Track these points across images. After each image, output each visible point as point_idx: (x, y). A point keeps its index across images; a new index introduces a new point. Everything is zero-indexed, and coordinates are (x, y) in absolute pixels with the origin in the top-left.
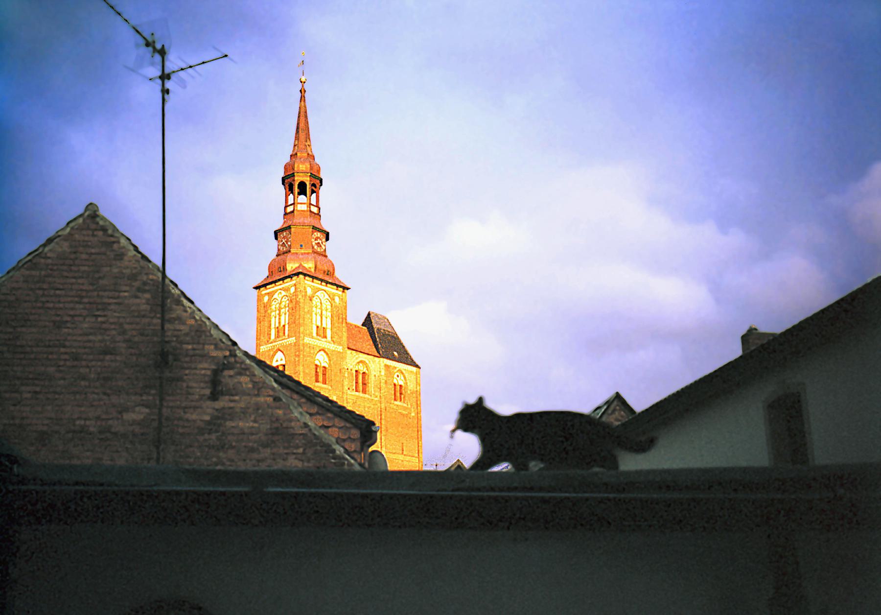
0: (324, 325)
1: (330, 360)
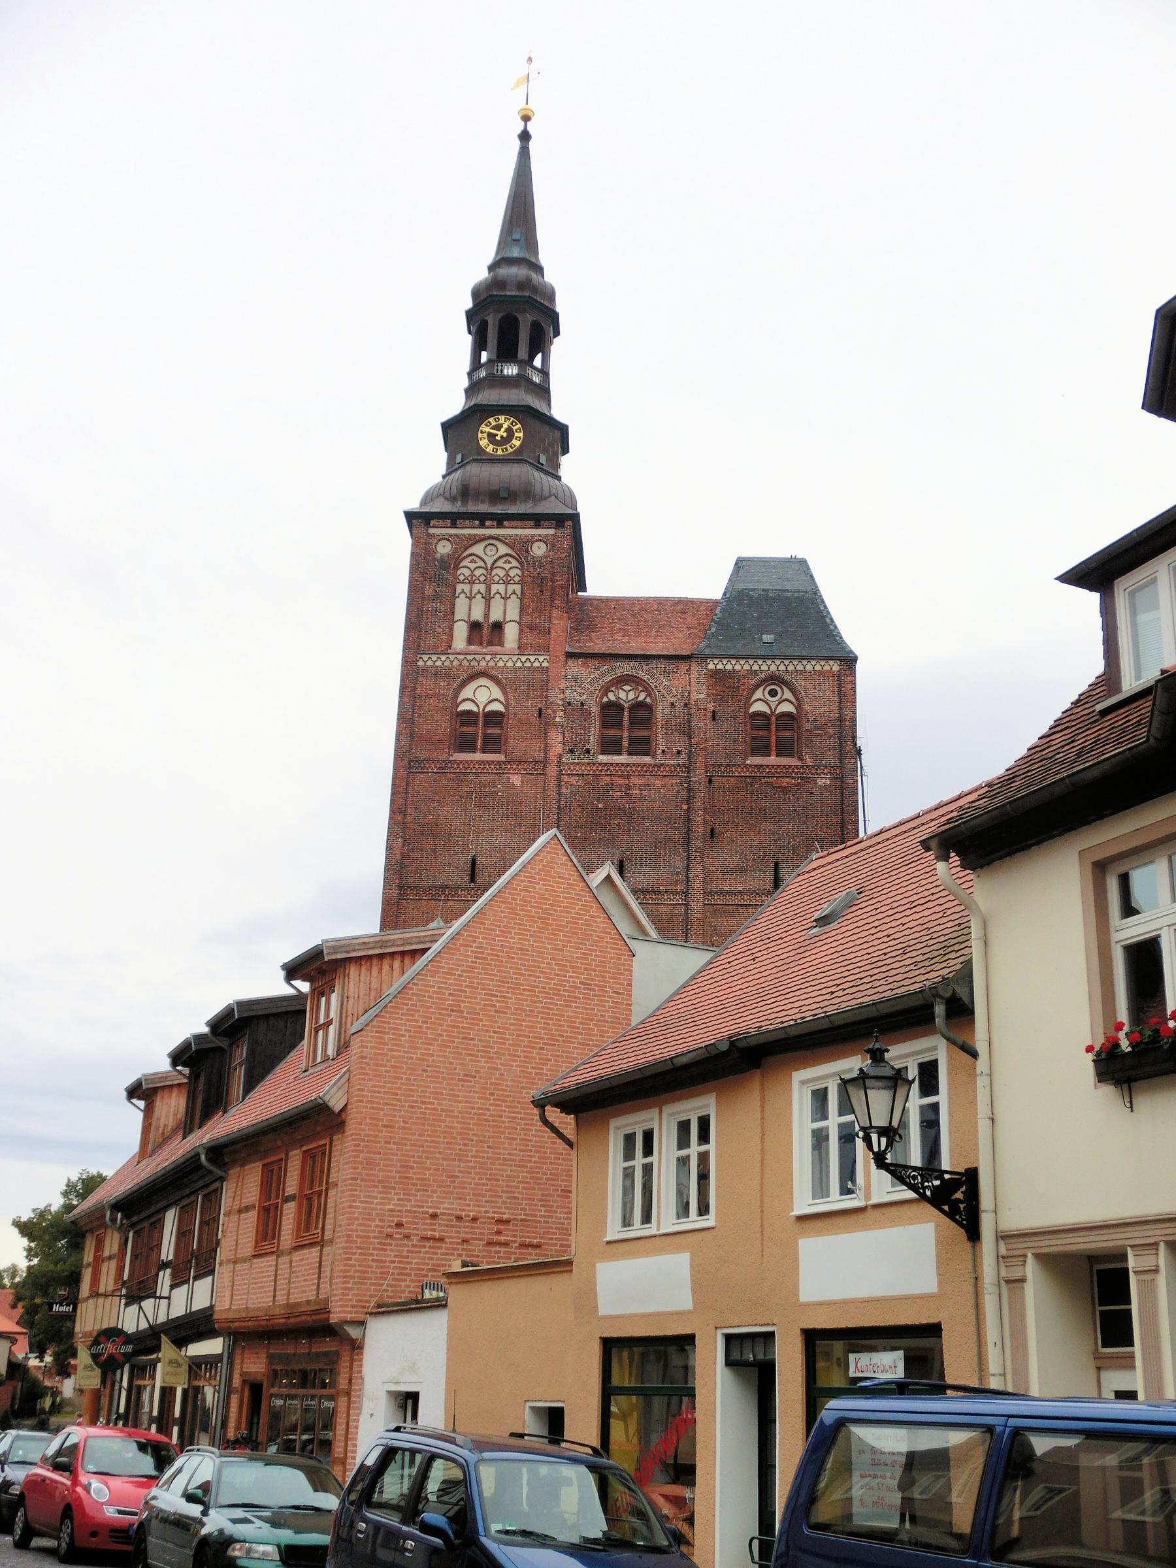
0: (496, 615)
1: (505, 694)
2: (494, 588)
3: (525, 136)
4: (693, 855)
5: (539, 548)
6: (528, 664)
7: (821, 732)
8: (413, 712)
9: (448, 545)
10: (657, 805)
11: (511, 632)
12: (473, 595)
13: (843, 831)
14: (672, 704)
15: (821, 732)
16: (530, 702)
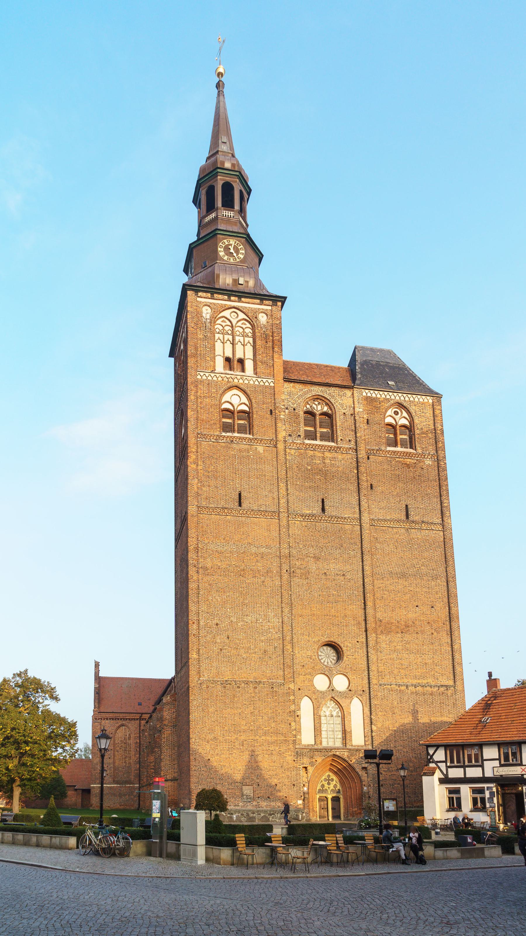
0: (239, 354)
1: (250, 400)
2: (237, 338)
4: (362, 498)
5: (263, 317)
6: (262, 383)
7: (425, 436)
8: (197, 406)
9: (209, 310)
10: (340, 469)
11: (249, 365)
12: (225, 341)
13: (440, 490)
14: (344, 414)
15: (425, 436)
16: (265, 406)
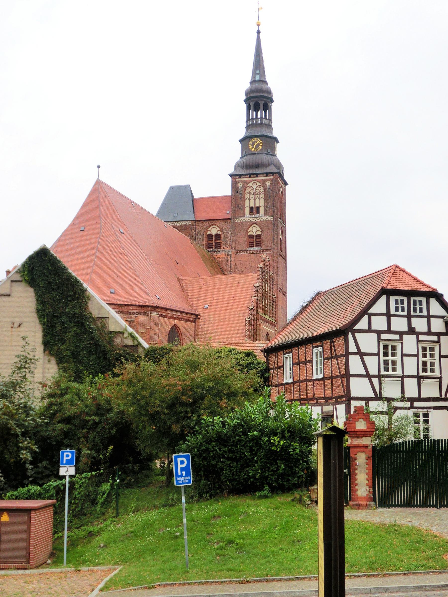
0: (257, 205)
2: (256, 196)
3: (259, 32)
11: (262, 210)
